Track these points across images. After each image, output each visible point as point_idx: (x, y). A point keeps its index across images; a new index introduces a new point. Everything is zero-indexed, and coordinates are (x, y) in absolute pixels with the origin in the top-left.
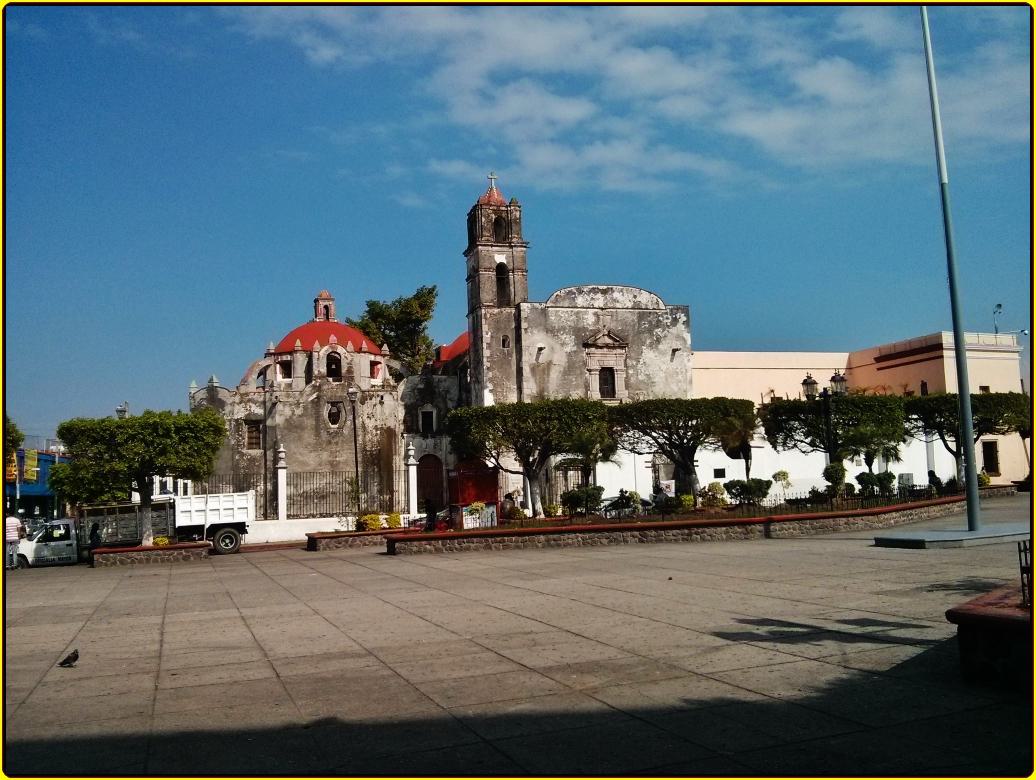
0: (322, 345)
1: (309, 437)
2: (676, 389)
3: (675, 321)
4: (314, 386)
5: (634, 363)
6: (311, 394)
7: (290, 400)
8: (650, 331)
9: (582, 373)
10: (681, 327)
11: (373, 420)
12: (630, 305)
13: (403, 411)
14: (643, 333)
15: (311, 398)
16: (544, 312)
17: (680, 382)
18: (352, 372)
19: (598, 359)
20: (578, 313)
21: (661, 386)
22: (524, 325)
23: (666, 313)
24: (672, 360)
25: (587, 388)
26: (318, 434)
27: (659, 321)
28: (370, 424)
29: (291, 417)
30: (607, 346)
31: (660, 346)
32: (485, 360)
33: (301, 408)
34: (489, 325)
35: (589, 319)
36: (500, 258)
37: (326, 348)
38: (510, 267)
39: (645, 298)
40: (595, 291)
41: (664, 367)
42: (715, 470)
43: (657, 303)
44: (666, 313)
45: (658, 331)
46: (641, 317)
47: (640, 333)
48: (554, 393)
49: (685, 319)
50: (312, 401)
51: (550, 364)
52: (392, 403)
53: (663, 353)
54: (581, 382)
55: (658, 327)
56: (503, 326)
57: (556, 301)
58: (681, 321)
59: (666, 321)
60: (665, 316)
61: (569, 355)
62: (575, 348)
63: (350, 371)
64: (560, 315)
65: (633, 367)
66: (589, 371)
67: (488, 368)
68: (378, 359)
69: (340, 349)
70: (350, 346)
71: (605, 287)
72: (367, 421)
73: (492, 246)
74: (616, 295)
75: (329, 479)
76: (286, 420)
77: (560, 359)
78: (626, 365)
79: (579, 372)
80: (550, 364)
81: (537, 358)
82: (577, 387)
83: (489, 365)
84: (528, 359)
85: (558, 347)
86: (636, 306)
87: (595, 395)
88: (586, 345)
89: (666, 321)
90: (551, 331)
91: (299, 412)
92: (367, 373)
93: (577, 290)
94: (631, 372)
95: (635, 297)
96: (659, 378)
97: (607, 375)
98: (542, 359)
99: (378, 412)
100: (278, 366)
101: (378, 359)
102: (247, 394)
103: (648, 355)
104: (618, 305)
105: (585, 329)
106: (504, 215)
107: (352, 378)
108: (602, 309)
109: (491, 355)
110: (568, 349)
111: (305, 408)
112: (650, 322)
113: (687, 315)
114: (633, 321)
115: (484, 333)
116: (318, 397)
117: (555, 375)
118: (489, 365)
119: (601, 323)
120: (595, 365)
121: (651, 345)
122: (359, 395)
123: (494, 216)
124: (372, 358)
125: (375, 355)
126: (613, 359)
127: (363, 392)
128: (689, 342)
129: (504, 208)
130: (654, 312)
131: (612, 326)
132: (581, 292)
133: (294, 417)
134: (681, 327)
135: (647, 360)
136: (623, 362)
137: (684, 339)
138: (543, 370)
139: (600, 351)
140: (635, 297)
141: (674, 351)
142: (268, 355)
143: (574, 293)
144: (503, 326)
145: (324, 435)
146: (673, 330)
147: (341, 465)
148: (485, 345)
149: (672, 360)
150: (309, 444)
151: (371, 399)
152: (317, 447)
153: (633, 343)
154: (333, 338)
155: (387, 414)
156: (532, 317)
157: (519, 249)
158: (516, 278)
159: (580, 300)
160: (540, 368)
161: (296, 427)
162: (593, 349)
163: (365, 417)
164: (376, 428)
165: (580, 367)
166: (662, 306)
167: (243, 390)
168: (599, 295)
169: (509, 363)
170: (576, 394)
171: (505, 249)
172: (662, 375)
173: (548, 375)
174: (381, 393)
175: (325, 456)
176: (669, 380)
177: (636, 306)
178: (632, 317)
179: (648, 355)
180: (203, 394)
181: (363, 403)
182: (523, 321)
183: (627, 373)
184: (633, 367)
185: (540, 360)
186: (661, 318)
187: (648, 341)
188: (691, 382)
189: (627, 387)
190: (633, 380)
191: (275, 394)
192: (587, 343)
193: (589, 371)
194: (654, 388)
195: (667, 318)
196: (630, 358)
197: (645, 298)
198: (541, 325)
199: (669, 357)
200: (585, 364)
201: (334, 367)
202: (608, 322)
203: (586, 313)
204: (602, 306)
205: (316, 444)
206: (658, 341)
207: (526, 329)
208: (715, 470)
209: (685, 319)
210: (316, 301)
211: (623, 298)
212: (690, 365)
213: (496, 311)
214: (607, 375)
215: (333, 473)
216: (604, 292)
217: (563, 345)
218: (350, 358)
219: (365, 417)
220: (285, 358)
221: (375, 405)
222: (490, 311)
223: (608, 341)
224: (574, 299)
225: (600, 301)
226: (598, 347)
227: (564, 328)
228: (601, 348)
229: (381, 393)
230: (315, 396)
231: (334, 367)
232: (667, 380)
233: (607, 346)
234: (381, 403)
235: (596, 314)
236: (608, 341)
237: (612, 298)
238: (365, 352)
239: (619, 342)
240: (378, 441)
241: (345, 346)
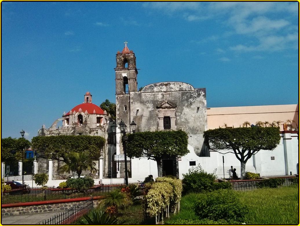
0: (76, 112)
2: (199, 124)
3: (199, 95)
5: (180, 114)
6: (72, 131)
8: (187, 100)
9: (156, 119)
10: (202, 97)
12: (178, 89)
13: (108, 136)
14: (184, 101)
15: (71, 132)
16: (140, 95)
17: (201, 121)
18: (87, 122)
19: (163, 113)
20: (154, 94)
21: (192, 123)
22: (131, 101)
23: (195, 92)
24: (197, 112)
25: (158, 125)
27: (191, 95)
30: (167, 107)
31: (192, 106)
32: (117, 115)
34: (119, 102)
35: (160, 96)
36: (125, 75)
37: (78, 113)
38: (128, 78)
39: (185, 86)
40: (162, 85)
41: (194, 115)
42: (190, 162)
43: (191, 88)
44: (195, 92)
45: (191, 100)
46: (183, 94)
47: (182, 101)
48: (144, 127)
49: (204, 94)
50: (72, 133)
51: (142, 116)
52: (101, 133)
53: (193, 109)
54: (155, 123)
55: (191, 98)
56: (124, 102)
57: (145, 90)
58: (202, 95)
59: (194, 95)
60: (194, 93)
61: (150, 112)
62: (153, 109)
63: (86, 121)
64: (147, 96)
65: (179, 116)
66: (159, 118)
67: (118, 119)
68: (101, 116)
69: (83, 114)
70: (86, 112)
71: (167, 83)
73: (121, 70)
74: (172, 86)
77: (146, 114)
78: (176, 115)
79: (154, 119)
80: (142, 116)
81: (137, 114)
82: (154, 125)
83: (118, 117)
84: (133, 114)
85: (145, 109)
86: (181, 90)
87: (161, 128)
88: (158, 108)
89: (194, 95)
90: (142, 102)
92: (96, 121)
93: (154, 85)
94: (178, 118)
95: (180, 86)
96: (191, 120)
97: (167, 120)
98: (139, 114)
100: (66, 120)
101: (101, 116)
102: (52, 131)
103: (186, 110)
104: (172, 90)
105: (157, 101)
106: (127, 57)
107: (86, 124)
108: (165, 92)
109: (120, 114)
110: (150, 110)
112: (187, 96)
113: (205, 92)
114: (179, 96)
115: (117, 105)
116: (74, 132)
117: (144, 121)
118: (118, 117)
119: (165, 98)
120: (161, 115)
121: (187, 106)
122: (89, 130)
123: (123, 58)
124: (98, 116)
125: (100, 115)
126: (170, 113)
127: (90, 129)
128: (206, 104)
129: (127, 55)
130: (190, 92)
131: (170, 99)
132: (156, 86)
134: (202, 97)
135: (185, 113)
136: (174, 114)
137: (203, 103)
138: (139, 119)
139: (164, 110)
140: (180, 86)
141: (198, 108)
142: (63, 116)
143: (153, 86)
144: (124, 102)
146: (198, 99)
148: (117, 110)
149: (197, 112)
151: (93, 132)
153: (179, 105)
154: (80, 109)
156: (134, 97)
157: (132, 70)
158: (130, 82)
159: (155, 89)
160: (138, 118)
162: (161, 109)
165: (155, 117)
166: (193, 89)
167: (51, 129)
168: (164, 86)
169: (127, 117)
170: (153, 129)
171: (127, 71)
172: (193, 119)
173: (141, 120)
174: (97, 129)
176: (196, 121)
177: (181, 90)
178: (179, 95)
179: (186, 110)
180: (40, 132)
182: (131, 99)
183: (176, 118)
184: (179, 116)
185: (138, 115)
186: (192, 94)
187: (186, 104)
188: (206, 121)
189: (176, 124)
190: (179, 121)
191: (60, 131)
192: (158, 106)
193: (159, 118)
194: (189, 125)
195: (195, 94)
196: (178, 112)
197: (185, 86)
198: (138, 100)
199: (196, 111)
200: (157, 115)
201: (81, 120)
202: (168, 97)
203: (158, 94)
204: (165, 91)
206: (191, 104)
207: (132, 102)
208: (190, 162)
209: (204, 94)
210: (91, 96)
211: (175, 87)
212: (206, 113)
213: (122, 96)
214: (167, 120)
216: (166, 85)
217: (148, 108)
218: (86, 116)
220: (67, 117)
222: (119, 96)
223: (167, 105)
224: (153, 89)
225: (164, 89)
226: (163, 108)
227: (148, 101)
228: (164, 108)
229: (97, 129)
230: (73, 131)
231: (81, 120)
232: (195, 121)
233: (167, 107)
235: (162, 94)
236: (167, 105)
237: (170, 87)
238: (94, 114)
239: (173, 105)
241: (84, 112)
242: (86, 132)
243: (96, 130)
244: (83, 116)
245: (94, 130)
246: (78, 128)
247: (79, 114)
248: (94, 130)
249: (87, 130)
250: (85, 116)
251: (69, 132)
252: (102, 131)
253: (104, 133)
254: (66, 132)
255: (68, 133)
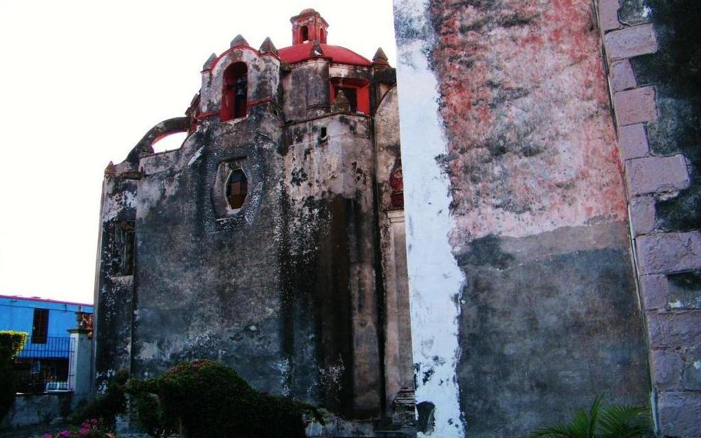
1: (184, 238)
4: (200, 135)
6: (192, 153)
7: (162, 169)
11: (304, 184)
15: (193, 160)
26: (200, 233)
28: (298, 194)
29: (159, 203)
33: (176, 183)
50: (194, 165)
52: (350, 140)
72: (292, 190)
75: (216, 327)
76: (152, 209)
91: (171, 190)
99: (315, 166)
111: (182, 182)
133: (164, 202)
145: (210, 230)
147: (240, 295)
150: (185, 253)
151: (300, 140)
152: (197, 259)
155: (333, 169)
161: (167, 220)
163: (287, 182)
164: (310, 202)
174: (320, 124)
175: (210, 275)
181: (283, 151)
205: (195, 252)
215: (227, 314)
218: (263, 66)
219: (287, 182)
221: (308, 152)
230: (198, 154)
234: (322, 143)
240: (314, 233)
242: (261, 151)
243: (315, 129)
244: (250, 67)
245: (305, 130)
246: (222, 135)
247: (230, 62)
248: (305, 130)
249: (267, 139)
250: (256, 67)
251: (182, 162)
252: (352, 128)
253: (365, 142)
254: (166, 165)
255: (177, 168)
